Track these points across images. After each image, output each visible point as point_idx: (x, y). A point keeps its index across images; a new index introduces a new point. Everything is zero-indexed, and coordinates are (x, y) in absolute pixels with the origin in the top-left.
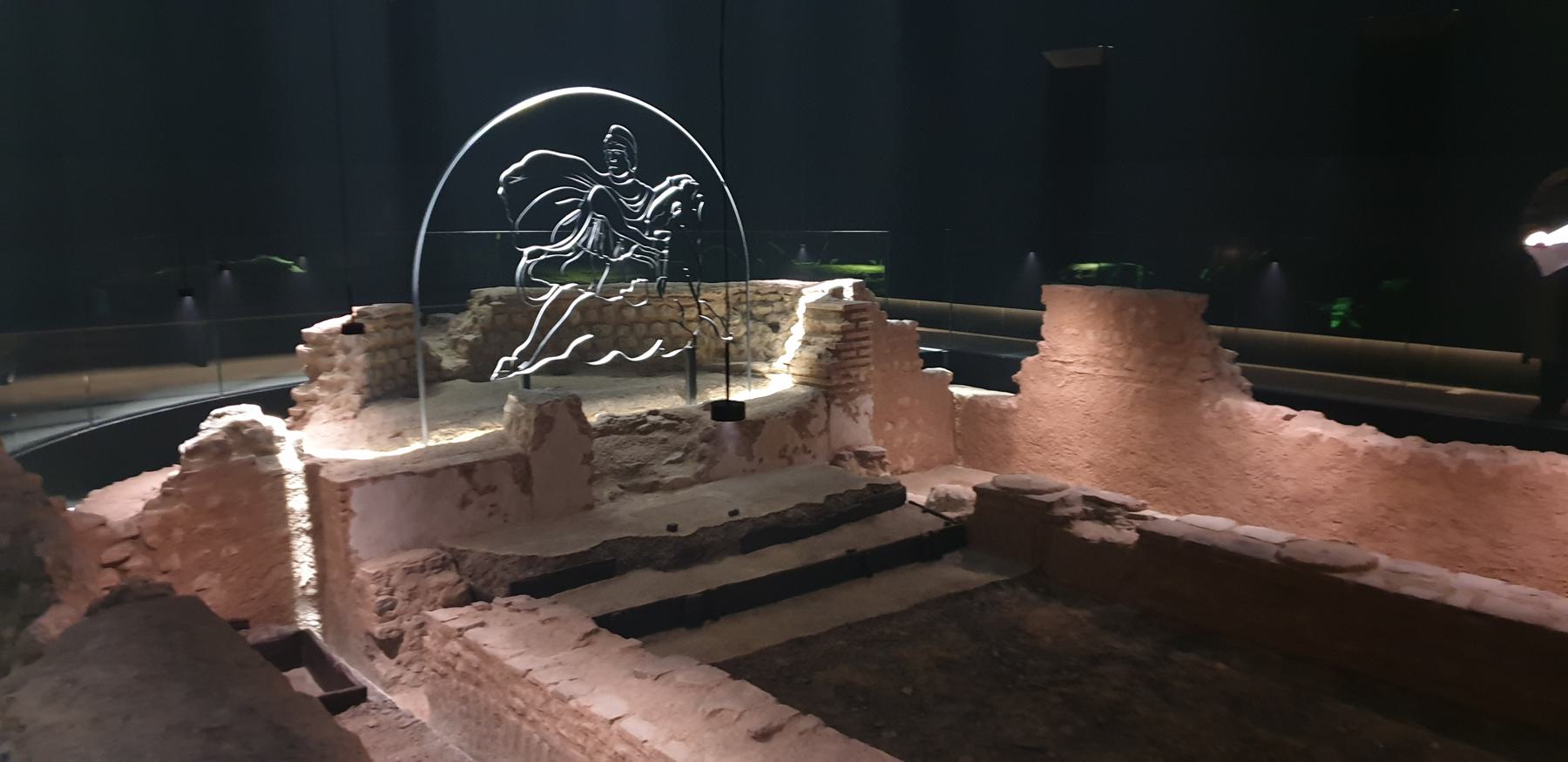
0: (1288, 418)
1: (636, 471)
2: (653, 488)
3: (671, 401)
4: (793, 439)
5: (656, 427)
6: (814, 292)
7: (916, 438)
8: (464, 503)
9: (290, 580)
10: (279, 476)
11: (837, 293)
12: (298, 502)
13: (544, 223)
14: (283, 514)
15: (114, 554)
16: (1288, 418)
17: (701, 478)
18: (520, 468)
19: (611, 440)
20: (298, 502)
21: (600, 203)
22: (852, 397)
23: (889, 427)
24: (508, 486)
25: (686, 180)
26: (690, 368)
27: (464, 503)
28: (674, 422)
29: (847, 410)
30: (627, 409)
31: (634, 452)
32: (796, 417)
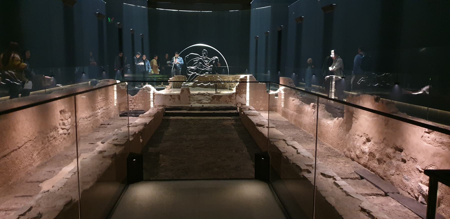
0: (293, 100)
1: (200, 100)
2: (201, 103)
3: (213, 92)
4: (228, 99)
5: (206, 95)
6: (242, 76)
7: (264, 104)
8: (170, 100)
9: (150, 107)
10: (150, 93)
11: (246, 77)
12: (152, 97)
13: (192, 64)
14: (150, 98)
15: (131, 99)
16: (293, 100)
17: (209, 103)
18: (179, 96)
19: (198, 96)
20: (152, 97)
21: (200, 61)
22: (242, 94)
23: (258, 102)
24: (177, 99)
25: (216, 57)
26: (216, 87)
27: (170, 100)
28: (209, 94)
29: (240, 96)
30: (202, 92)
31: (202, 98)
32: (230, 96)
